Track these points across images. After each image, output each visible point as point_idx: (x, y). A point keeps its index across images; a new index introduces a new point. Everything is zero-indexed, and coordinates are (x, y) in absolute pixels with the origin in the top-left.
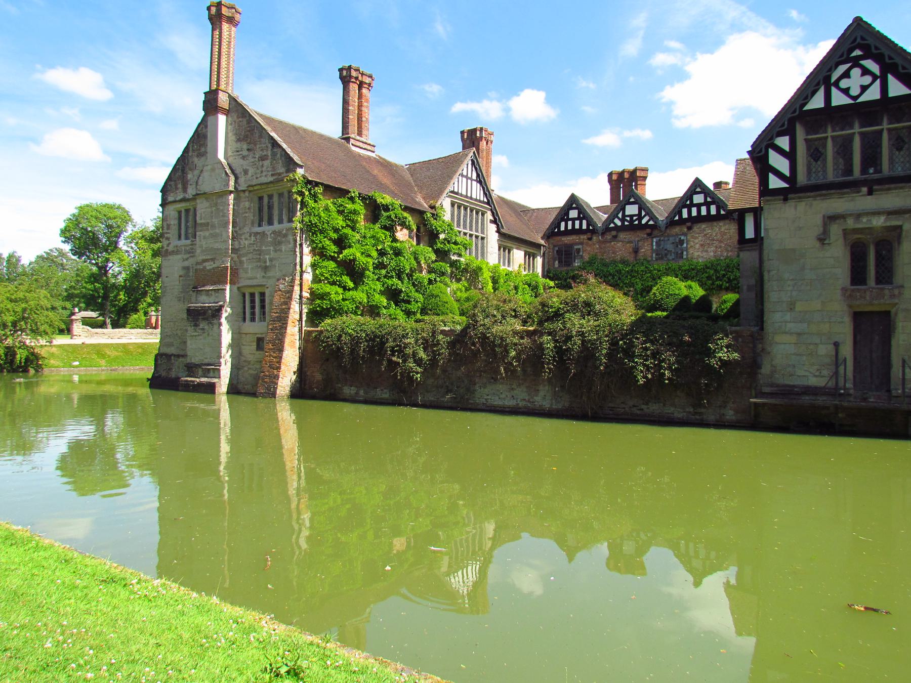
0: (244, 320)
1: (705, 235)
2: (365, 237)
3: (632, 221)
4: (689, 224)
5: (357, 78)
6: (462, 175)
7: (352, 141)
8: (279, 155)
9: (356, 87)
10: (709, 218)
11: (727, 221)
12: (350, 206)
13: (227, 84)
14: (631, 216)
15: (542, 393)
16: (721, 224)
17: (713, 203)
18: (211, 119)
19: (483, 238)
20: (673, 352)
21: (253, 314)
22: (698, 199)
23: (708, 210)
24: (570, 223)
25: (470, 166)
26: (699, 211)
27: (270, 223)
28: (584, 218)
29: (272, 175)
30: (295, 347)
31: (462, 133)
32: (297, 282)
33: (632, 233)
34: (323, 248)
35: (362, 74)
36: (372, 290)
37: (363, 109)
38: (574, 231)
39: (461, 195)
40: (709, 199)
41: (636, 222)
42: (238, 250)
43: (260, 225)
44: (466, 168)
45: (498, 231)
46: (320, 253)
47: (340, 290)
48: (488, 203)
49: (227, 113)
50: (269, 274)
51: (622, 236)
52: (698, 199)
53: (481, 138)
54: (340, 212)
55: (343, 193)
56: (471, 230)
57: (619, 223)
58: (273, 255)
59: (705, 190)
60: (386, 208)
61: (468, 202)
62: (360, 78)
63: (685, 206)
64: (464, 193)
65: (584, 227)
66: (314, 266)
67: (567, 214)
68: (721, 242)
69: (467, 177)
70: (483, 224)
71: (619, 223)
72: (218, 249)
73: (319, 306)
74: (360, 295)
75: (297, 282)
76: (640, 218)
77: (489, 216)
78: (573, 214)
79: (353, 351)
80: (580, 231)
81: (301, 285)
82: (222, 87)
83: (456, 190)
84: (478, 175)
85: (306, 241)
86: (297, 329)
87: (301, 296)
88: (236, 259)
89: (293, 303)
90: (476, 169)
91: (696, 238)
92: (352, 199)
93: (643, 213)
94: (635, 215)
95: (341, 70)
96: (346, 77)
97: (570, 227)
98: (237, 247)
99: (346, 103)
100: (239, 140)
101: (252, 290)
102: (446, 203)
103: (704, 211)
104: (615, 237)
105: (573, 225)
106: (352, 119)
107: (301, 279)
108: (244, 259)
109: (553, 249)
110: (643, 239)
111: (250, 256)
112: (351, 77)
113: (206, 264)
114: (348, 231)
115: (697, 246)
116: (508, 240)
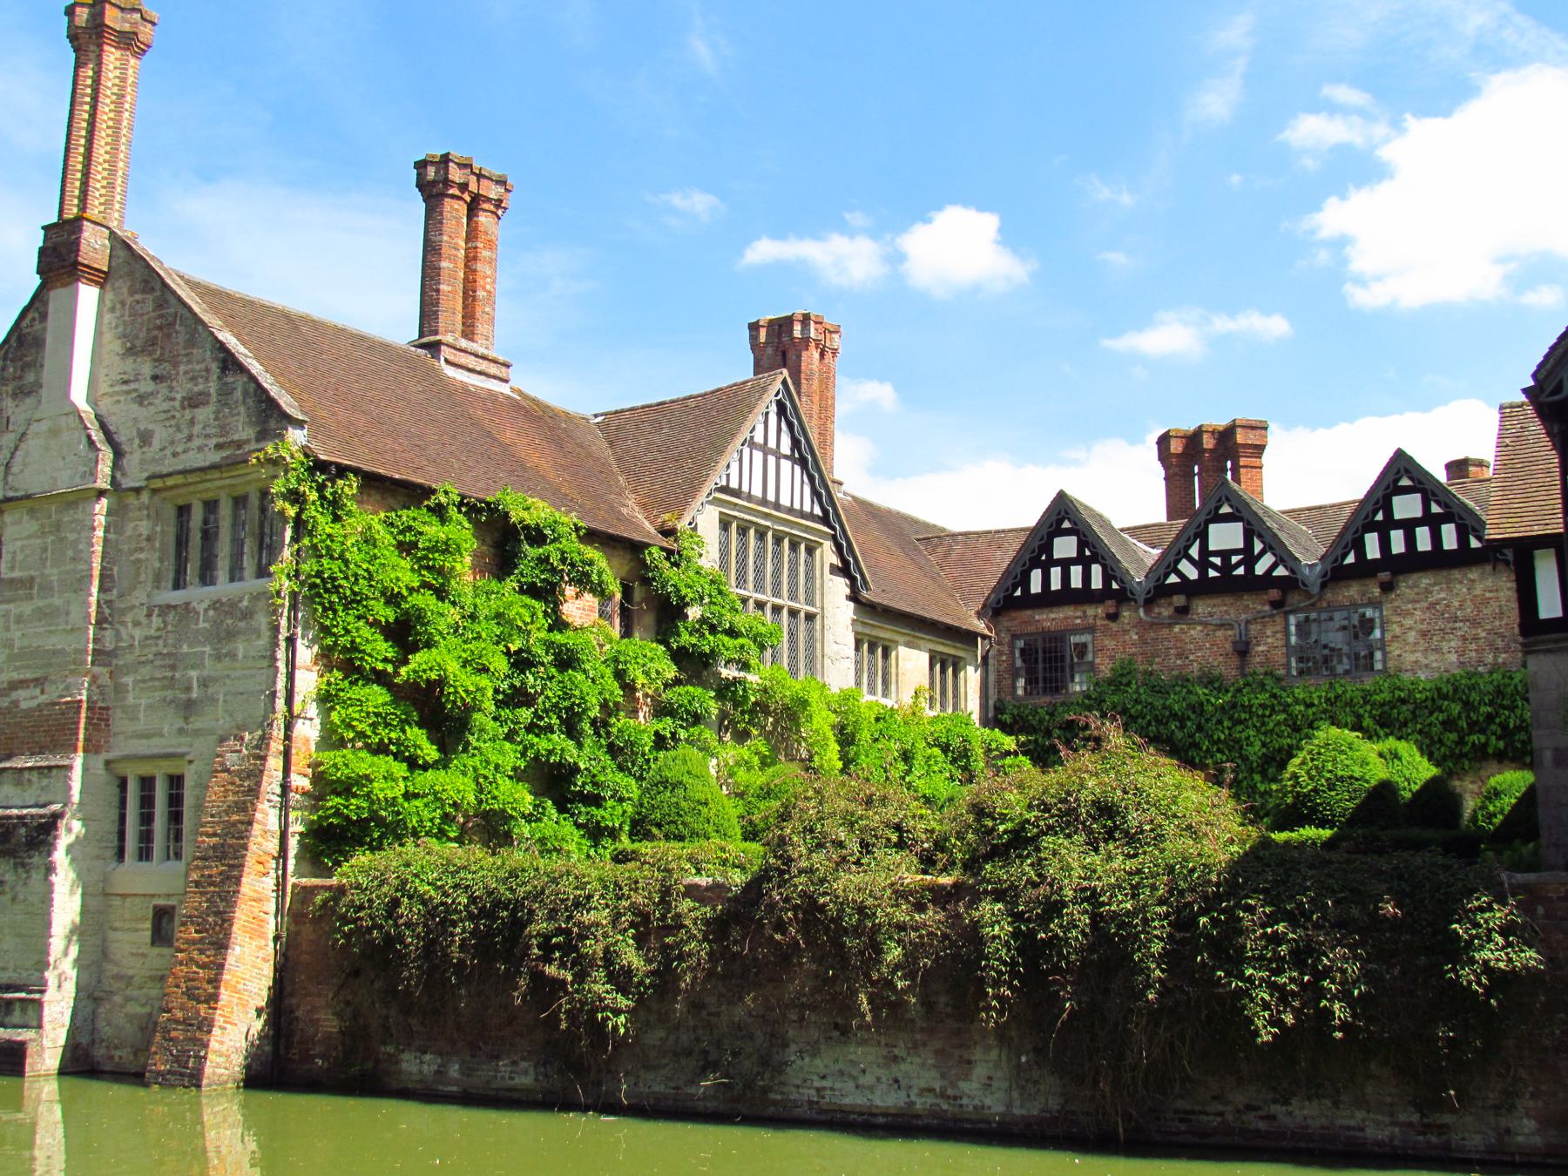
0: (120, 854)
1: (1432, 606)
2: (473, 617)
3: (1227, 568)
4: (1384, 576)
5: (464, 187)
6: (752, 444)
7: (445, 352)
8: (238, 394)
9: (462, 208)
10: (1438, 560)
12: (433, 530)
13: (108, 204)
14: (1225, 555)
15: (980, 1071)
16: (1473, 574)
17: (1447, 518)
18: (56, 296)
19: (810, 617)
20: (1352, 947)
21: (146, 837)
22: (1407, 506)
23: (1436, 538)
24: (1056, 572)
25: (773, 418)
26: (1410, 540)
27: (207, 577)
28: (1095, 558)
29: (219, 447)
30: (262, 935)
31: (754, 327)
32: (276, 746)
34: (354, 648)
35: (480, 176)
36: (492, 766)
37: (479, 266)
38: (1067, 596)
39: (749, 497)
40: (1435, 509)
41: (1240, 571)
42: (112, 654)
43: (178, 584)
44: (763, 425)
45: (854, 597)
46: (344, 662)
47: (400, 769)
48: (825, 520)
49: (102, 279)
50: (198, 723)
51: (1201, 607)
52: (1407, 506)
53: (806, 340)
54: (406, 548)
55: (414, 494)
56: (777, 593)
57: (1192, 573)
58: (210, 668)
59: (1422, 484)
60: (537, 536)
61: (767, 516)
62: (473, 187)
63: (1371, 526)
64: (757, 492)
65: (1097, 583)
66: (326, 699)
67: (1048, 547)
68: (1475, 623)
69: (764, 448)
70: (810, 577)
71: (1192, 573)
72: (55, 652)
73: (338, 813)
74: (456, 784)
75: (276, 746)
76: (1250, 559)
77: (827, 555)
79: (432, 946)
80: (1085, 596)
81: (287, 755)
82: (94, 212)
83: (734, 484)
84: (795, 443)
85: (306, 628)
86: (270, 882)
87: (285, 787)
88: (105, 680)
89: (263, 806)
90: (790, 426)
91: (1409, 614)
92: (439, 512)
93: (1258, 546)
94: (1236, 552)
95: (421, 166)
96: (434, 183)
97: (1056, 584)
98: (109, 646)
99: (431, 249)
100: (131, 351)
101: (146, 769)
102: (707, 520)
103: (1423, 541)
104: (1183, 611)
105: (1066, 577)
106: (448, 294)
107: (288, 737)
108: (128, 680)
109: (1012, 646)
110: (1260, 618)
111: (145, 671)
112: (447, 183)
113: (21, 694)
114: (426, 600)
115: (1412, 636)
116: (882, 622)
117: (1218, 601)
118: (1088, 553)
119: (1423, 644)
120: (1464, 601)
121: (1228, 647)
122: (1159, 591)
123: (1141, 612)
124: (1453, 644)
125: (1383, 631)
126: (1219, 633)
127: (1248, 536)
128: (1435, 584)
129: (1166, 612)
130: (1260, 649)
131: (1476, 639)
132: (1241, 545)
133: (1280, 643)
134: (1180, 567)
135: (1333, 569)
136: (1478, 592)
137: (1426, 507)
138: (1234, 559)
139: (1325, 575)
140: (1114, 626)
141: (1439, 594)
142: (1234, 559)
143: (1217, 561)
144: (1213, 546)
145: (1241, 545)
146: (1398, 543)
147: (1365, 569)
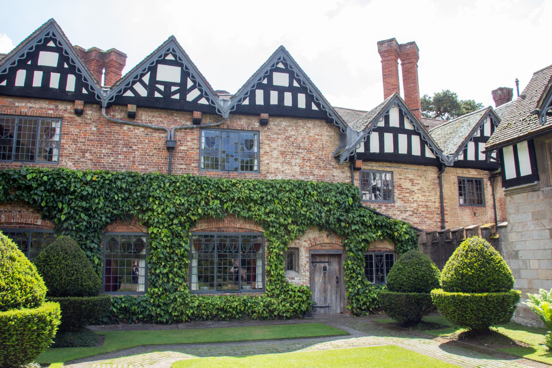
1: (288, 138)
3: (167, 93)
4: (265, 116)
11: (318, 123)
14: (168, 85)
16: (310, 124)
17: (303, 89)
23: (295, 100)
26: (281, 98)
28: (73, 70)
33: (164, 115)
38: (45, 93)
40: (296, 84)
51: (144, 117)
63: (260, 86)
65: (71, 86)
67: (34, 56)
68: (309, 151)
71: (143, 92)
76: (184, 90)
78: (48, 59)
80: (60, 95)
93: (190, 84)
94: (175, 84)
97: (37, 81)
103: (288, 101)
104: (132, 116)
115: (275, 153)
117: (156, 114)
118: (66, 66)
119: (281, 159)
120: (304, 138)
121: (161, 144)
122: (119, 101)
123: (104, 111)
124: (298, 161)
125: (259, 148)
126: (156, 135)
127: (185, 74)
128: (289, 126)
129: (119, 115)
130: (182, 148)
131: (309, 160)
132: (178, 81)
133: (195, 146)
134: (134, 87)
135: (237, 105)
136: (311, 134)
137: (291, 83)
138: (174, 89)
139: (233, 108)
140: (78, 119)
141: (291, 132)
142: (174, 89)
143: (162, 88)
144: (158, 79)
145: (178, 81)
146: (274, 99)
147: (252, 111)
